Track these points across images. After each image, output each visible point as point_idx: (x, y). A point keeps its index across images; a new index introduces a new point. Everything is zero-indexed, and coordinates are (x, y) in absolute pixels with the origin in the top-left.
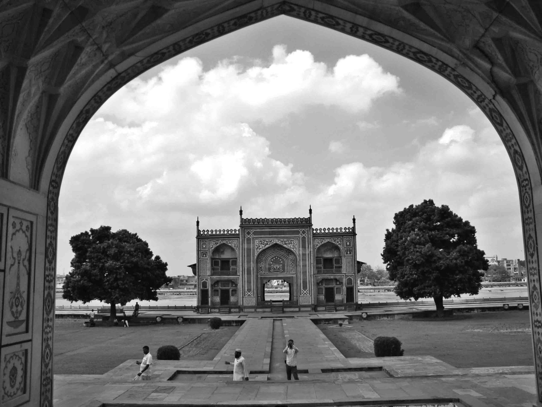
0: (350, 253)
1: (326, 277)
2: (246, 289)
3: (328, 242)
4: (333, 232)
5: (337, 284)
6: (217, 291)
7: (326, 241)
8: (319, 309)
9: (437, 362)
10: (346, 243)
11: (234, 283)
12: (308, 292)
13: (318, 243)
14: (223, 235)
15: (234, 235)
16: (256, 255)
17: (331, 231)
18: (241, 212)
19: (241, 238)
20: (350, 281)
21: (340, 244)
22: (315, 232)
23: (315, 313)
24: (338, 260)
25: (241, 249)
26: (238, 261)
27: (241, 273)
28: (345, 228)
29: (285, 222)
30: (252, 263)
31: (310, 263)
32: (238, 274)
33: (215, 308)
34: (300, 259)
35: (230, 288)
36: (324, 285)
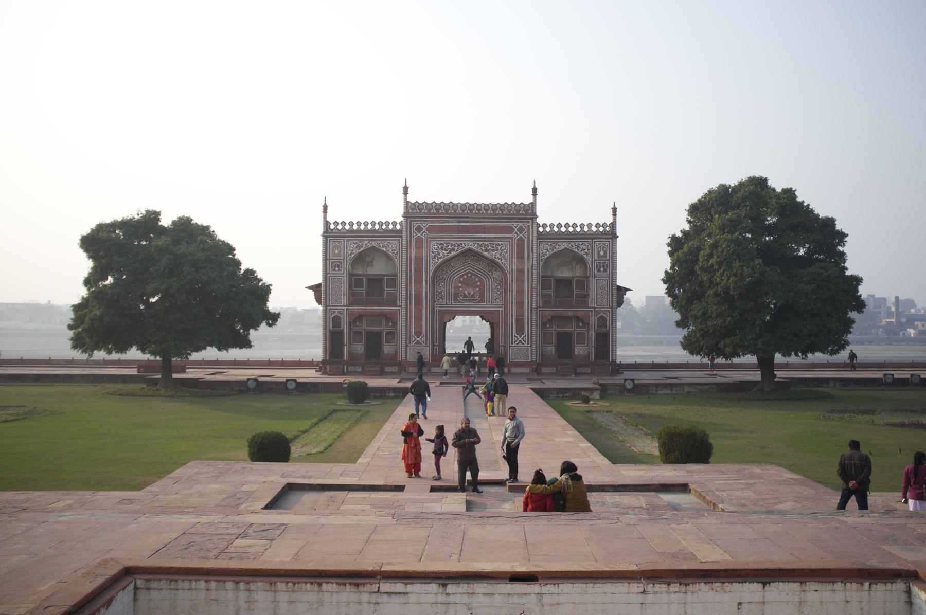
0: (605, 271)
2: (413, 330)
3: (566, 249)
4: (575, 231)
5: (578, 327)
6: (361, 333)
7: (562, 247)
8: (545, 370)
9: (793, 479)
10: (599, 252)
11: (391, 319)
13: (547, 249)
14: (371, 231)
15: (392, 231)
17: (571, 229)
18: (406, 189)
19: (404, 237)
20: (602, 322)
21: (587, 254)
22: (541, 229)
23: (536, 377)
24: (583, 283)
25: (404, 258)
26: (399, 279)
27: (404, 301)
28: (598, 225)
29: (486, 210)
30: (424, 283)
31: (531, 285)
33: (354, 365)
34: (512, 278)
35: (384, 328)
36: (555, 327)
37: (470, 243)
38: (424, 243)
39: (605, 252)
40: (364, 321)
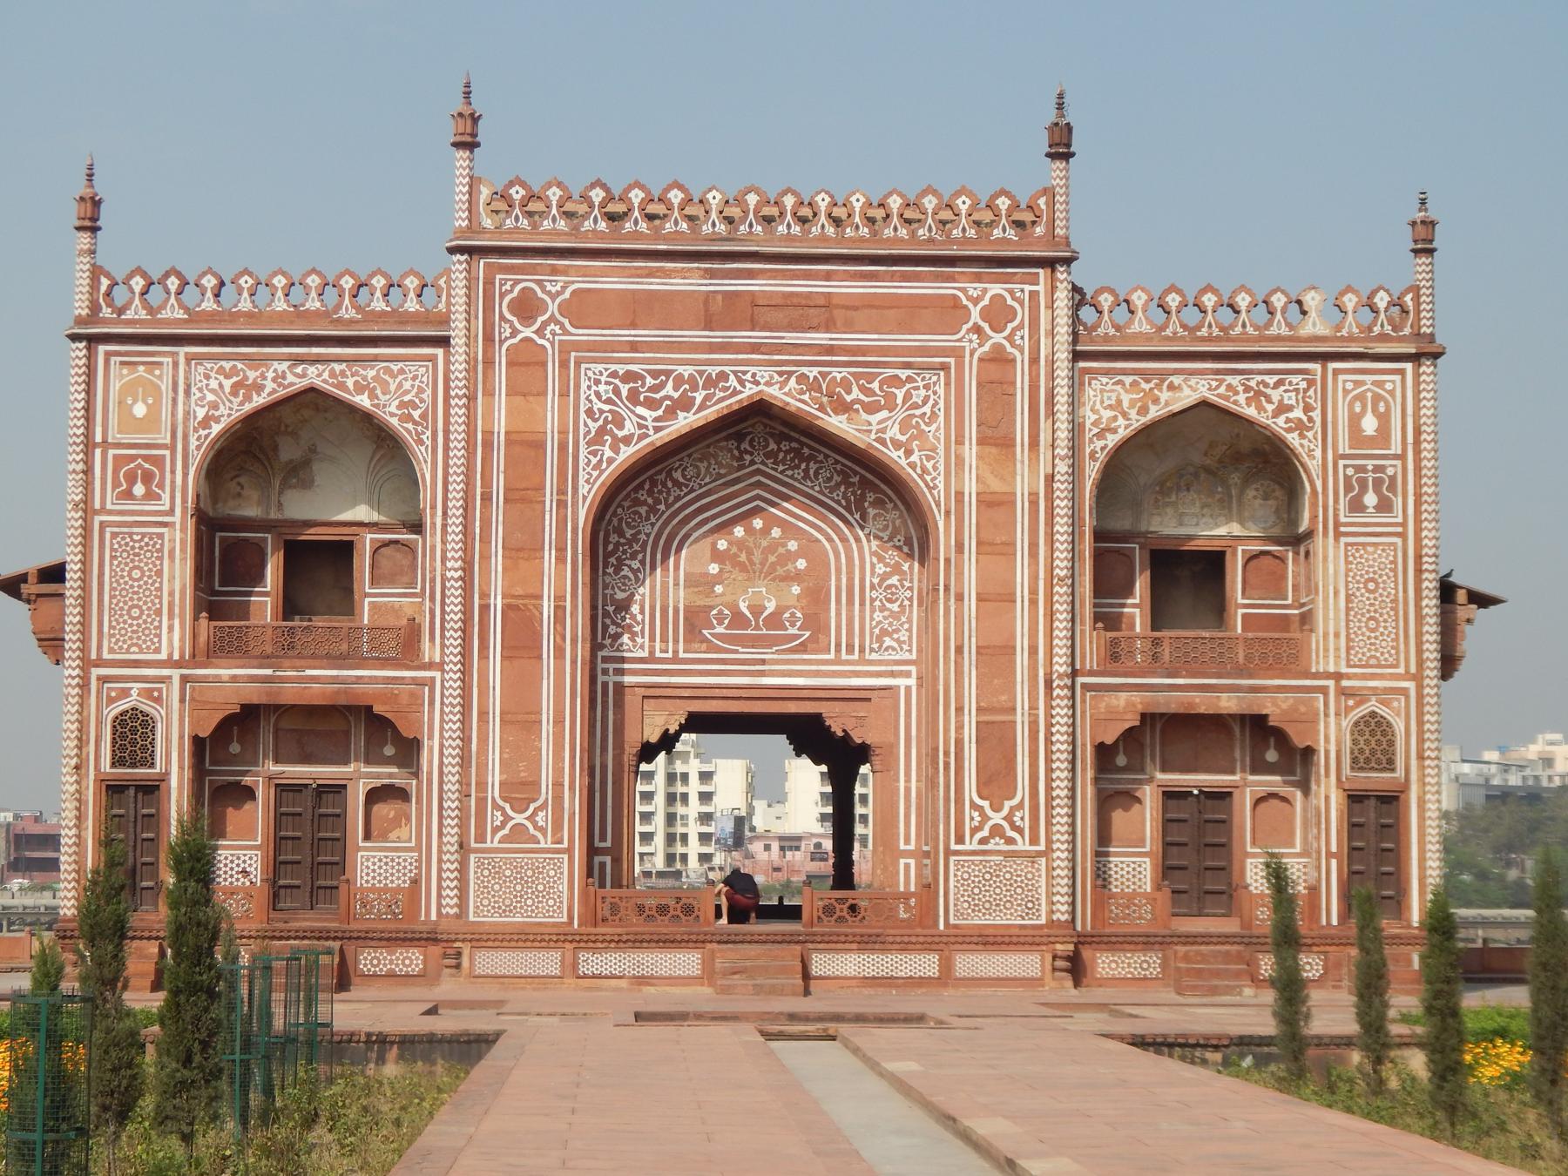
0: (1384, 506)
1: (1171, 703)
2: (495, 777)
3: (1204, 404)
5: (1259, 767)
8: (1105, 964)
10: (1355, 421)
12: (1023, 818)
13: (1116, 408)
16: (589, 490)
19: (458, 342)
20: (1374, 742)
21: (1300, 427)
27: (454, 639)
30: (549, 556)
32: (430, 651)
37: (764, 373)
38: (552, 370)
39: (1384, 419)
40: (266, 737)
